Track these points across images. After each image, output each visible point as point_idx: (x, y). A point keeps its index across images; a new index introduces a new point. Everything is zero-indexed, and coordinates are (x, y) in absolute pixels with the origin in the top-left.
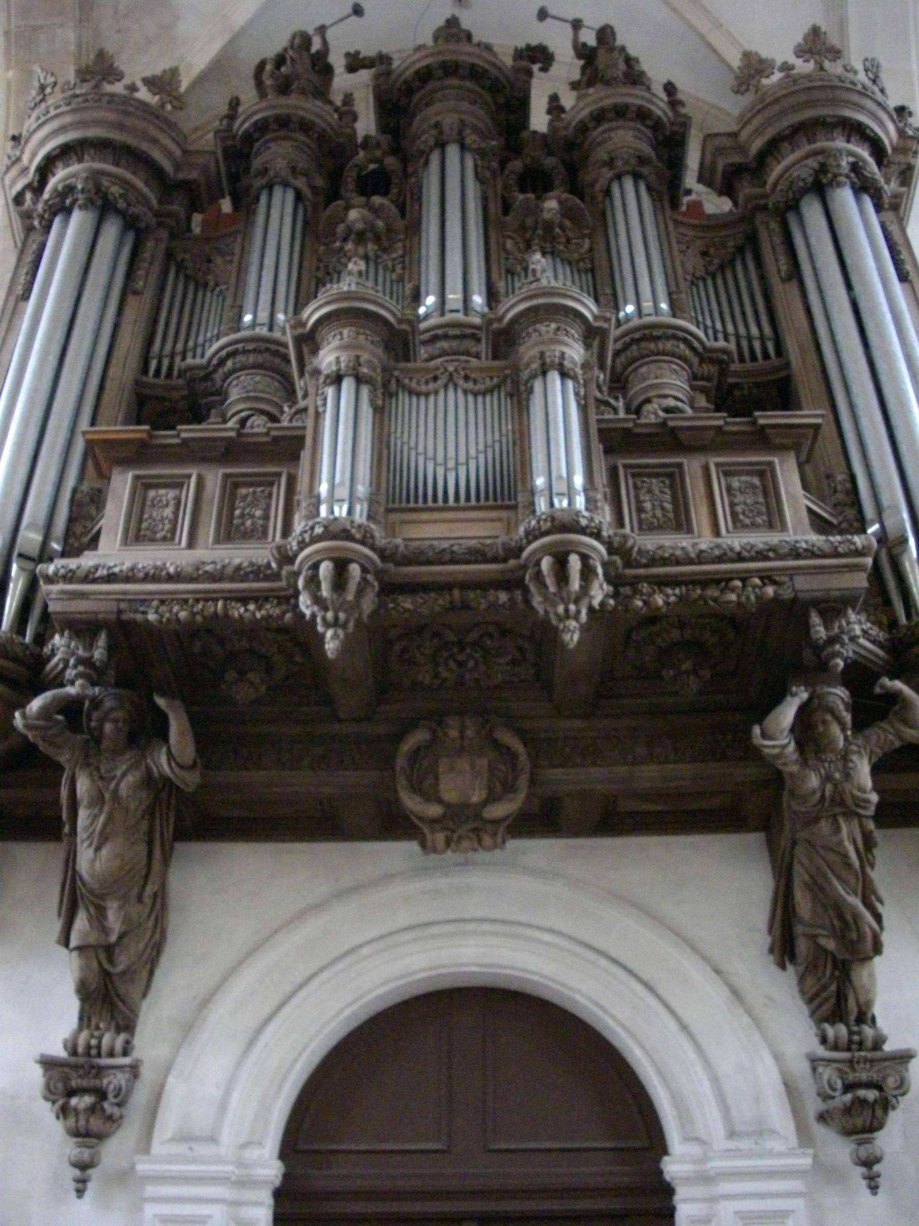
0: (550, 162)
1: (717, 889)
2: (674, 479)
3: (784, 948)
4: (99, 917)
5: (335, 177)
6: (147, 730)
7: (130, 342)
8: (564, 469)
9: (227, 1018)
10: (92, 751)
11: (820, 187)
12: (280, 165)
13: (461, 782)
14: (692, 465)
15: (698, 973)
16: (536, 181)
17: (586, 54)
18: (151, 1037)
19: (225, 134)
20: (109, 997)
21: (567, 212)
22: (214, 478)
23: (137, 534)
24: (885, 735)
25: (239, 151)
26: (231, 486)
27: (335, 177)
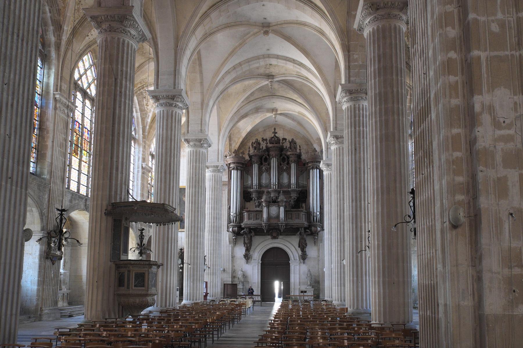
0: (285, 157)
1: (295, 240)
2: (291, 214)
3: (299, 247)
4: (247, 245)
5: (261, 159)
6: (250, 232)
7: (242, 186)
8: (282, 215)
9: (257, 251)
10: (246, 234)
11: (313, 168)
12: (255, 161)
13: (275, 234)
14: (293, 213)
15: (293, 247)
16: (284, 160)
17: (290, 143)
18: (251, 252)
19: (249, 154)
20: (248, 250)
21: (287, 167)
22: (255, 213)
23: (249, 219)
24: (307, 233)
25: (250, 157)
26: (256, 214)
27: (261, 159)
